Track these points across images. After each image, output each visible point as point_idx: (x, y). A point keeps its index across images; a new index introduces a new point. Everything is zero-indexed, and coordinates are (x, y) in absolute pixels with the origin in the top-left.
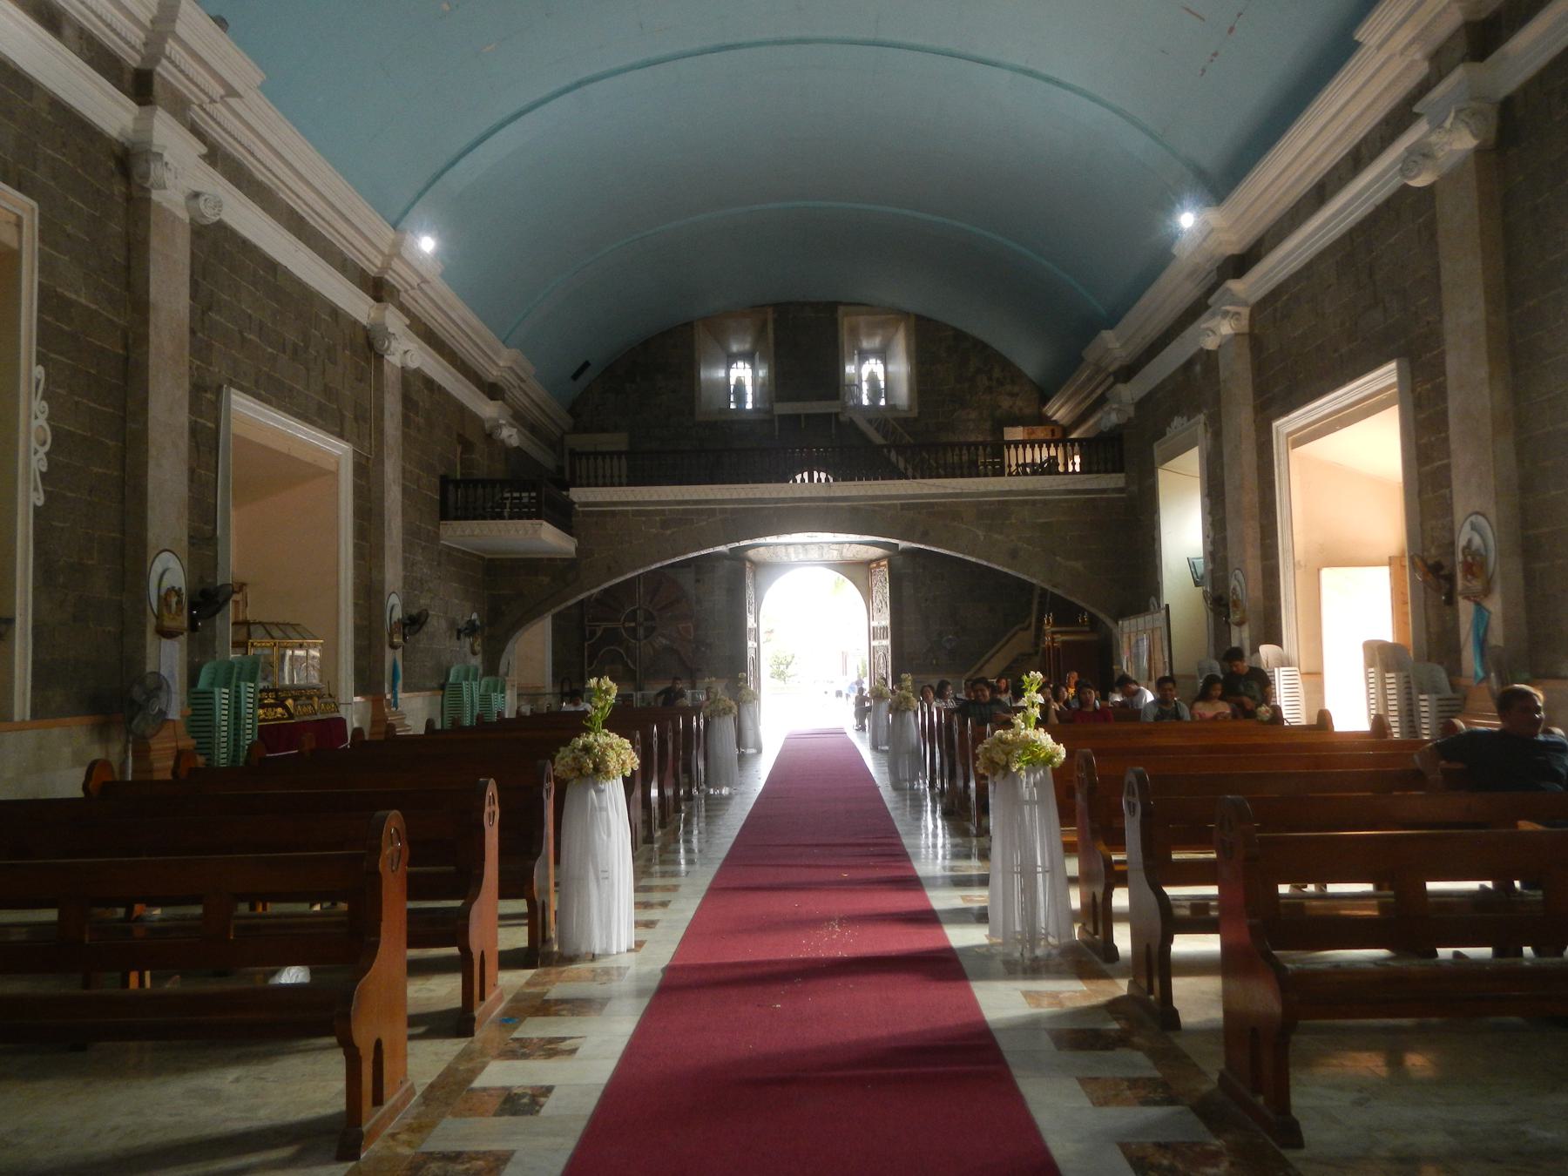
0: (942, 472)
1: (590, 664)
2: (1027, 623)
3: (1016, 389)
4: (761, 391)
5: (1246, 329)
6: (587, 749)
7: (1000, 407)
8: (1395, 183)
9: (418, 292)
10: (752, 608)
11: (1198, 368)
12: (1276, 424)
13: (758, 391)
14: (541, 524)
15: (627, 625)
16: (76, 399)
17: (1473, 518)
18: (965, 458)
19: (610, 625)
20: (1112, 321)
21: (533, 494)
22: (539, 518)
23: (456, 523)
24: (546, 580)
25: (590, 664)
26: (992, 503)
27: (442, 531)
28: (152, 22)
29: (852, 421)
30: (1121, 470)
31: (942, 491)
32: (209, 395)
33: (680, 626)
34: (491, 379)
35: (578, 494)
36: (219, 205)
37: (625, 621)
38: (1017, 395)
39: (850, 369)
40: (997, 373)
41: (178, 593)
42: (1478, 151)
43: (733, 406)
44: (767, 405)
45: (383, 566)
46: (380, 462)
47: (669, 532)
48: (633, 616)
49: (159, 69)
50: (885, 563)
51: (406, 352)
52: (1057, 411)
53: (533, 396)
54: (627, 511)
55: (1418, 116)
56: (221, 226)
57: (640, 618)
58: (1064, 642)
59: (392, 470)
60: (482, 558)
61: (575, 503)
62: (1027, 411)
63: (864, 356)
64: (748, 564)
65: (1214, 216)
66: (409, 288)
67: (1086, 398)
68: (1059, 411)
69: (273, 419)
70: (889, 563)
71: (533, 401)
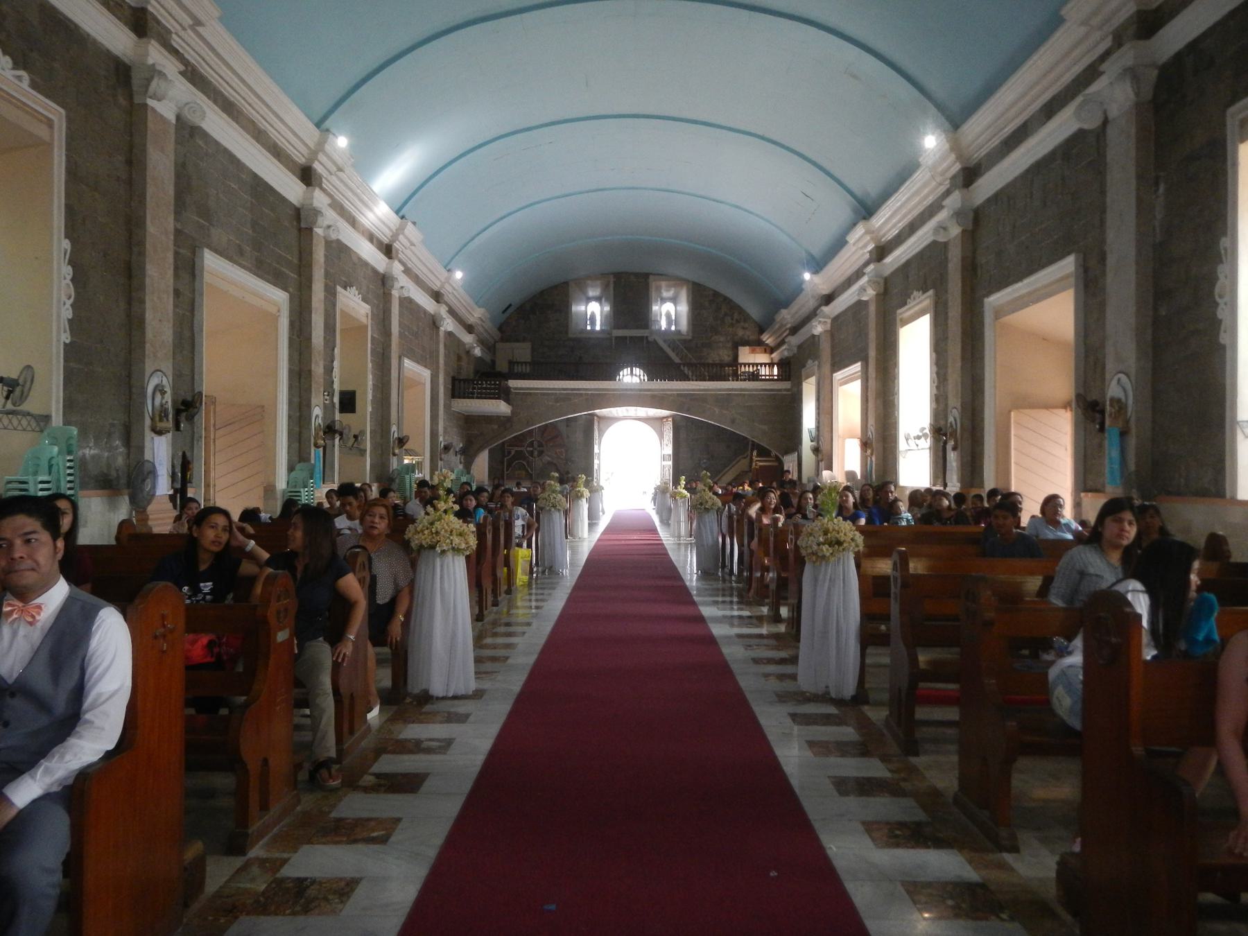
2: (745, 455)
3: (746, 325)
4: (605, 319)
6: (579, 491)
7: (737, 335)
8: (855, 299)
10: (597, 442)
12: (834, 375)
13: (603, 321)
15: (528, 449)
19: (520, 449)
20: (786, 304)
22: (500, 399)
24: (496, 427)
26: (723, 395)
28: (396, 230)
29: (655, 340)
30: (789, 380)
31: (698, 388)
33: (558, 451)
34: (470, 323)
35: (513, 383)
36: (409, 291)
37: (527, 447)
38: (746, 328)
39: (655, 308)
40: (736, 316)
42: (877, 295)
43: (589, 328)
44: (609, 329)
47: (558, 404)
48: (531, 444)
49: (395, 244)
50: (670, 419)
52: (768, 339)
53: (486, 327)
57: (536, 444)
58: (761, 466)
62: (753, 337)
63: (663, 300)
64: (596, 418)
65: (817, 279)
67: (779, 337)
68: (768, 339)
70: (673, 420)
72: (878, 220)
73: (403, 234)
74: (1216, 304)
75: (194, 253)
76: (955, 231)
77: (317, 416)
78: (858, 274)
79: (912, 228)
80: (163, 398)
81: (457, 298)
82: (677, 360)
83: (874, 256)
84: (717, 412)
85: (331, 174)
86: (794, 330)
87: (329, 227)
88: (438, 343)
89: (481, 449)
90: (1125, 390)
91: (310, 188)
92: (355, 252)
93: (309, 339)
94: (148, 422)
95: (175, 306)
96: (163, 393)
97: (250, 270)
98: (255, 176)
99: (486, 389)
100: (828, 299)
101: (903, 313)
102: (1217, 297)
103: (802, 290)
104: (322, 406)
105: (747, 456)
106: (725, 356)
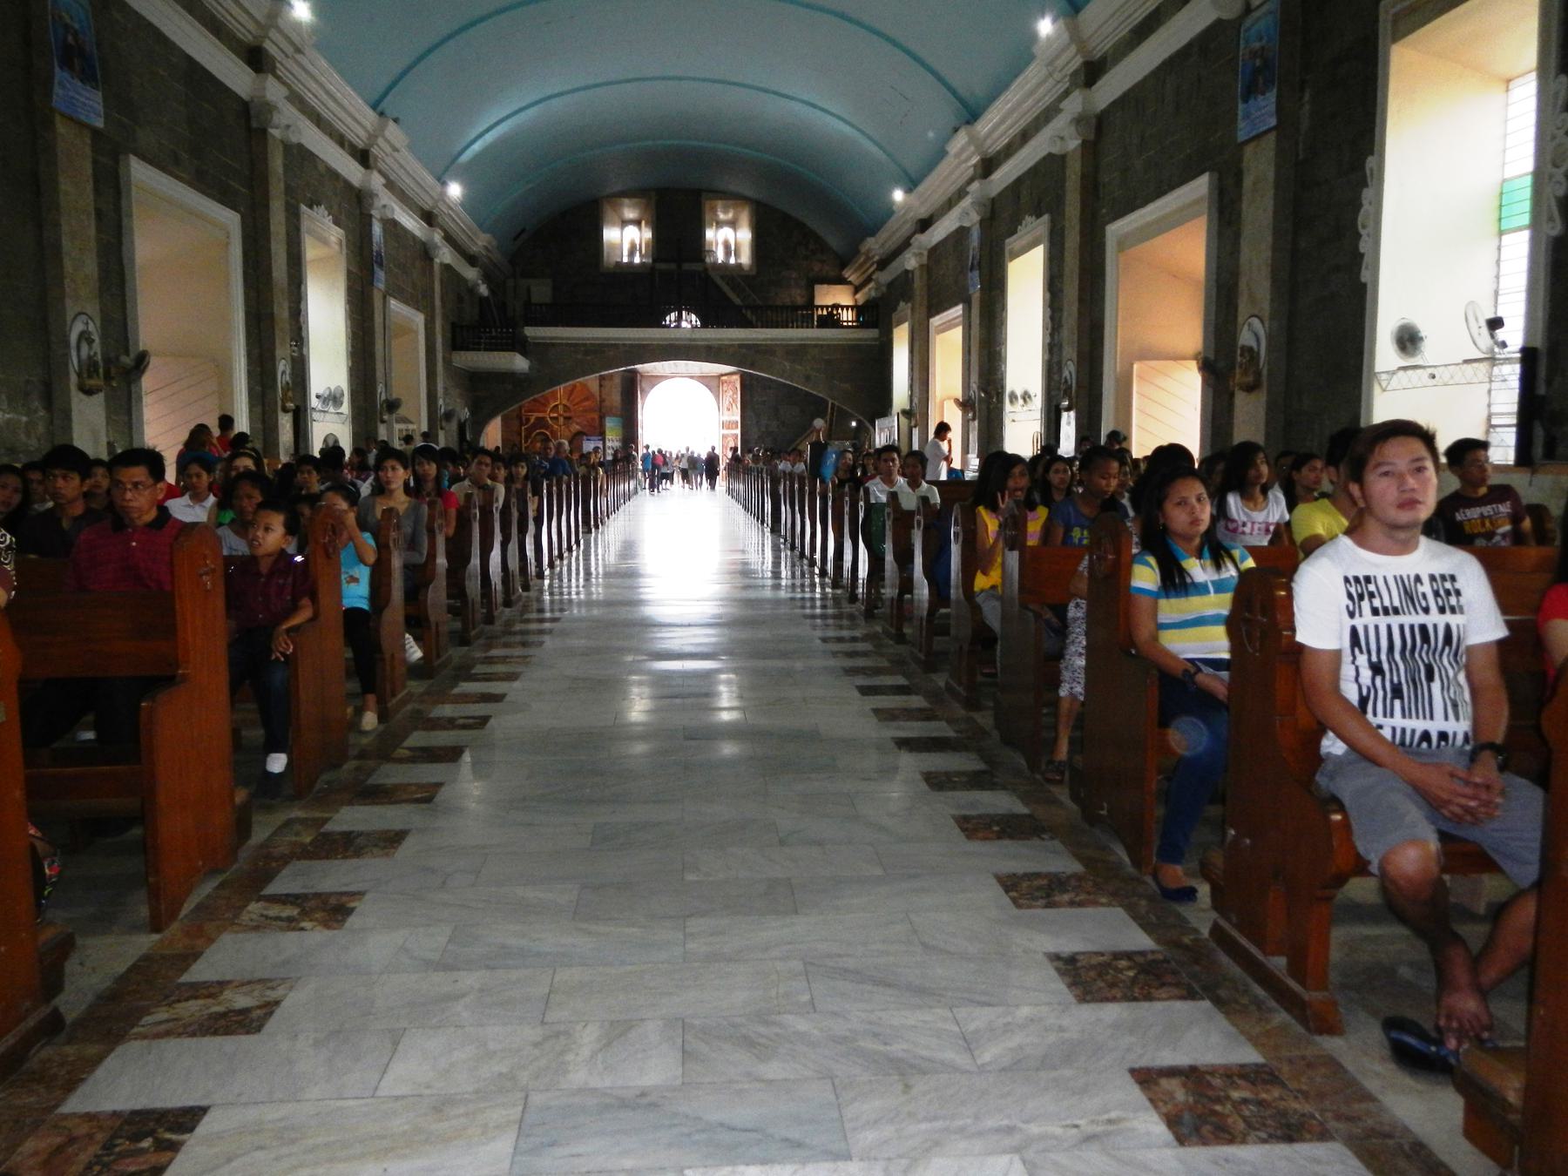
1: (526, 442)
12: (931, 320)
15: (552, 415)
19: (541, 415)
20: (873, 232)
35: (530, 332)
36: (393, 210)
38: (824, 261)
39: (710, 234)
44: (650, 261)
47: (589, 358)
52: (853, 273)
55: (968, 193)
60: (468, 372)
61: (527, 337)
62: (832, 274)
63: (720, 224)
67: (864, 273)
68: (852, 275)
72: (983, 126)
73: (383, 137)
74: (1359, 236)
75: (117, 162)
76: (1073, 144)
77: (284, 372)
78: (961, 194)
79: (1025, 136)
80: (90, 348)
82: (737, 301)
83: (980, 171)
85: (287, 56)
86: (883, 264)
87: (288, 127)
89: (491, 416)
90: (1258, 340)
91: (261, 75)
92: (323, 161)
93: (269, 272)
94: (74, 378)
95: (99, 230)
96: (90, 342)
97: (190, 184)
98: (190, 59)
99: (493, 338)
100: (925, 224)
101: (1011, 243)
102: (1360, 227)
104: (289, 359)
106: (798, 297)
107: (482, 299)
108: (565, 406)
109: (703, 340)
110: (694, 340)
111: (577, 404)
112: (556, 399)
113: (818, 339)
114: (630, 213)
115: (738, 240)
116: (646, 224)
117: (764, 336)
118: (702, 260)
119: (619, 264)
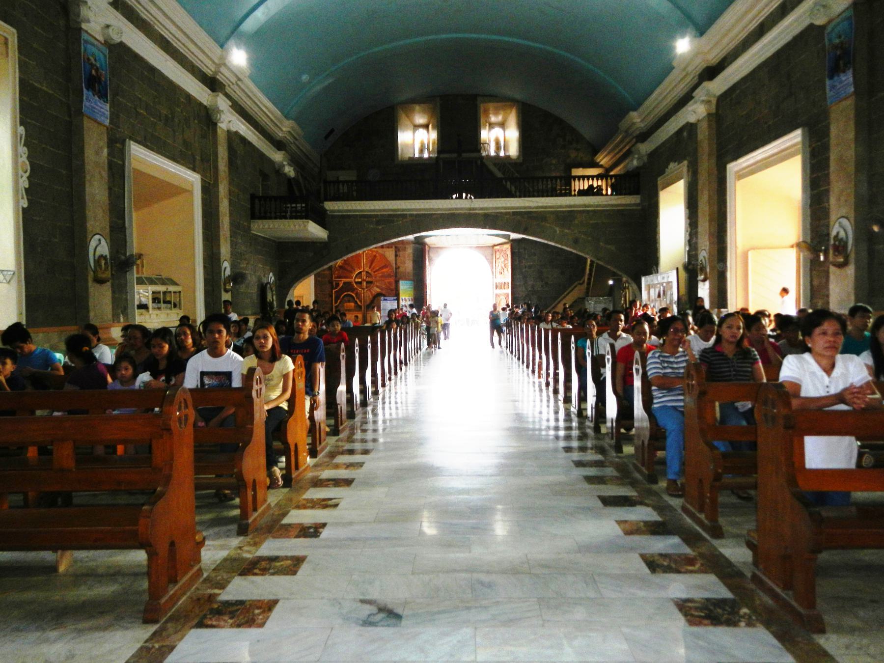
0: (536, 194)
1: (336, 303)
2: (581, 282)
5: (714, 111)
8: (806, 23)
9: (236, 86)
11: (685, 134)
14: (308, 222)
15: (357, 280)
16: (44, 146)
17: (841, 220)
18: (549, 186)
21: (304, 205)
22: (307, 217)
23: (260, 221)
24: (311, 254)
25: (336, 303)
27: (252, 226)
32: (118, 145)
34: (278, 138)
35: (330, 206)
36: (121, 33)
37: (355, 278)
41: (105, 258)
45: (219, 245)
46: (216, 184)
51: (230, 122)
52: (601, 160)
54: (357, 215)
56: (121, 45)
59: (223, 189)
60: (274, 241)
61: (327, 210)
63: (492, 126)
64: (427, 246)
66: (231, 84)
68: (604, 159)
69: (155, 159)
71: (303, 152)
81: (272, 120)
84: (558, 232)
88: (215, 144)
100: (711, 72)
103: (672, 68)
105: (584, 282)
107: (289, 180)
108: (367, 272)
109: (482, 209)
110: (474, 209)
111: (377, 271)
112: (360, 268)
113: (585, 206)
114: (420, 119)
115: (507, 138)
116: (433, 128)
117: (535, 205)
118: (479, 151)
119: (412, 159)
